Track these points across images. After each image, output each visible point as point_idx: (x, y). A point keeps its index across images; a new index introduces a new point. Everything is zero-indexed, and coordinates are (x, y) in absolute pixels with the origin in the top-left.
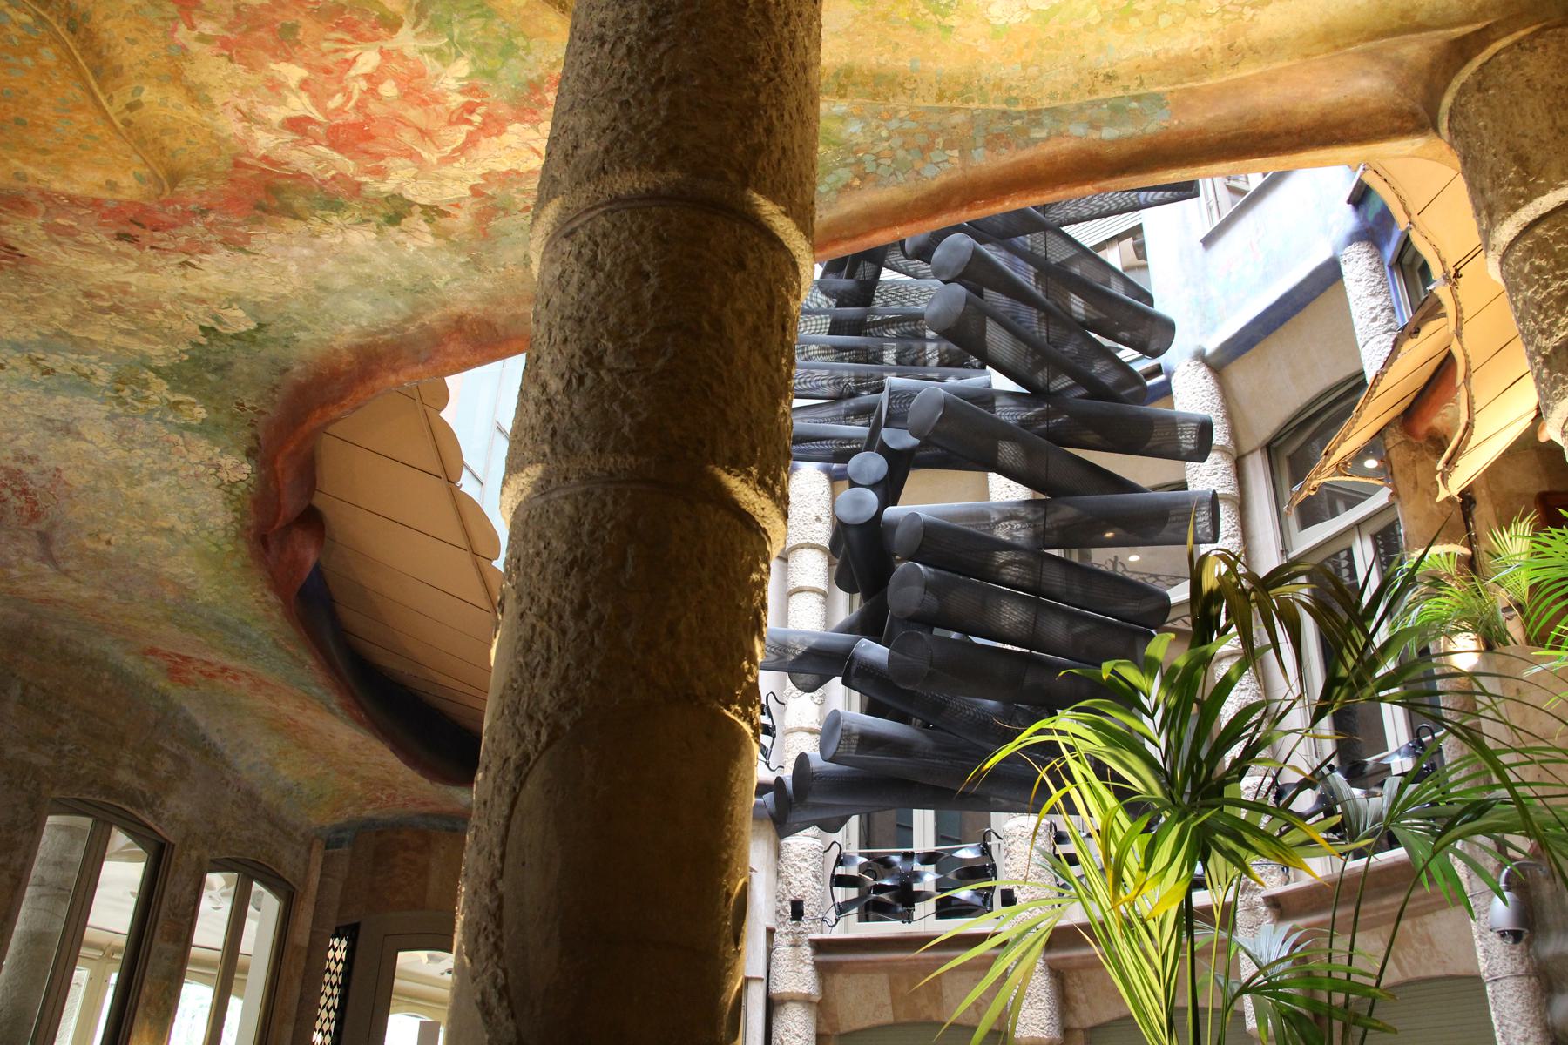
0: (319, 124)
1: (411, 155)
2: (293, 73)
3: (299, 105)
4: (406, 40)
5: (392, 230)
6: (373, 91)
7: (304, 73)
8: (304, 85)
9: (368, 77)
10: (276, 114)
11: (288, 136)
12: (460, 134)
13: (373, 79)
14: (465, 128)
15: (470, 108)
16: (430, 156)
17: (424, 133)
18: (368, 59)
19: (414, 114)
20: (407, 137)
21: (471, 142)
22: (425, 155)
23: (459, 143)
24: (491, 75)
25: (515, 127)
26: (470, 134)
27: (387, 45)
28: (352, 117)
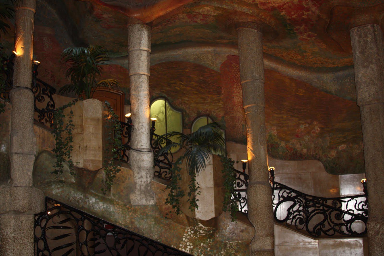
0: (305, 11)
1: (293, 4)
2: (304, 17)
3: (306, 13)
4: (288, 17)
6: (295, 13)
7: (303, 17)
8: (304, 15)
9: (295, 15)
10: (310, 12)
12: (285, 6)
14: (283, 7)
15: (282, 10)
16: (290, 4)
18: (294, 17)
19: (290, 10)
20: (293, 7)
21: (283, 5)
22: (291, 4)
23: (285, 5)
25: (276, 6)
26: (283, 6)
27: (290, 18)
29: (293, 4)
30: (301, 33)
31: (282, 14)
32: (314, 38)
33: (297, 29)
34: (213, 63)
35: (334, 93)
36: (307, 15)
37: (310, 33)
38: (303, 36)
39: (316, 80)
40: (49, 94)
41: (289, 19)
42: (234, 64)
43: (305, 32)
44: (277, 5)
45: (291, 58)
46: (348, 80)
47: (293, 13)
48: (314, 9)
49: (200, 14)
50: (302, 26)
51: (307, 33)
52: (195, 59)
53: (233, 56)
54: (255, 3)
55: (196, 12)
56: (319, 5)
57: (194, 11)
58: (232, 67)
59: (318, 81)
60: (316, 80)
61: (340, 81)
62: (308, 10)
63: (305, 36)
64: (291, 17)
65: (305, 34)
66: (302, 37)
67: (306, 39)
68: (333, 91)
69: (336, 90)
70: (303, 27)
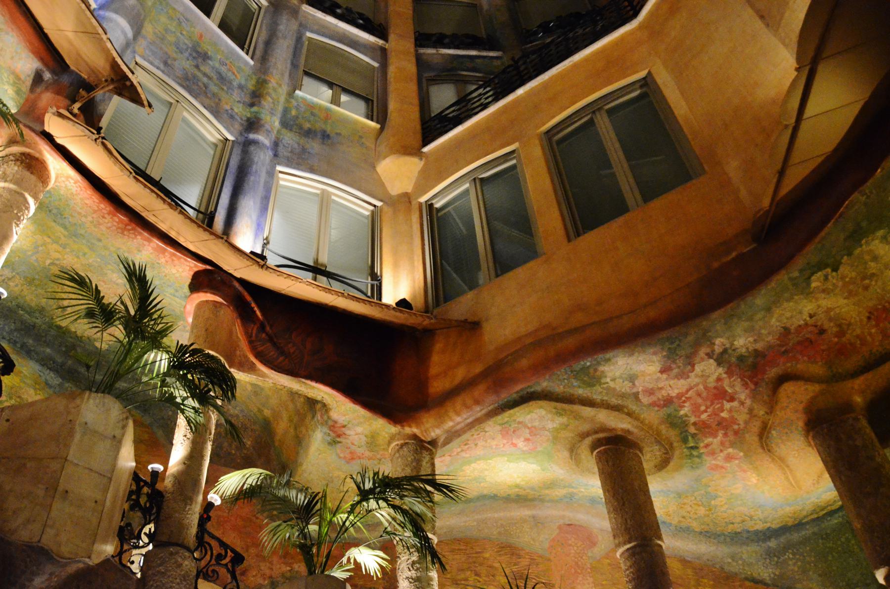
2: (724, 415)
3: (727, 405)
4: (693, 419)
5: (728, 346)
6: (707, 408)
8: (723, 411)
11: (737, 396)
13: (705, 411)
15: (684, 402)
16: (701, 387)
17: (699, 395)
18: (704, 416)
20: (704, 394)
21: (688, 391)
24: (676, 410)
28: (716, 402)
29: (706, 388)
30: (713, 453)
31: (682, 413)
32: (737, 462)
33: (707, 446)
34: (533, 540)
35: (769, 582)
36: (730, 411)
37: (730, 450)
38: (715, 459)
39: (730, 560)
40: (230, 566)
41: (695, 424)
42: (573, 540)
43: (721, 451)
44: (676, 391)
45: (684, 517)
46: (791, 556)
47: (703, 408)
48: (743, 397)
49: (526, 426)
50: (715, 436)
51: (725, 452)
52: (500, 533)
53: (569, 525)
54: (635, 390)
55: (519, 423)
56: (752, 387)
57: (515, 420)
58: (570, 545)
59: (733, 560)
60: (730, 560)
61: (776, 559)
62: (732, 399)
63: (720, 460)
64: (699, 417)
65: (721, 454)
66: (713, 462)
67: (722, 467)
68: (768, 578)
69: (772, 576)
70: (719, 438)
